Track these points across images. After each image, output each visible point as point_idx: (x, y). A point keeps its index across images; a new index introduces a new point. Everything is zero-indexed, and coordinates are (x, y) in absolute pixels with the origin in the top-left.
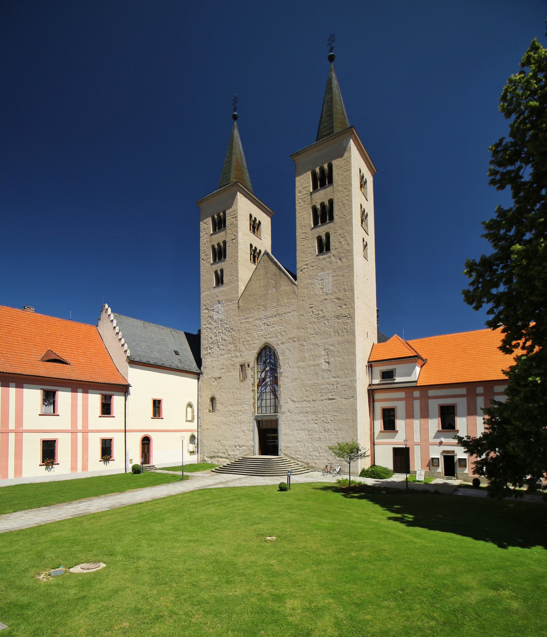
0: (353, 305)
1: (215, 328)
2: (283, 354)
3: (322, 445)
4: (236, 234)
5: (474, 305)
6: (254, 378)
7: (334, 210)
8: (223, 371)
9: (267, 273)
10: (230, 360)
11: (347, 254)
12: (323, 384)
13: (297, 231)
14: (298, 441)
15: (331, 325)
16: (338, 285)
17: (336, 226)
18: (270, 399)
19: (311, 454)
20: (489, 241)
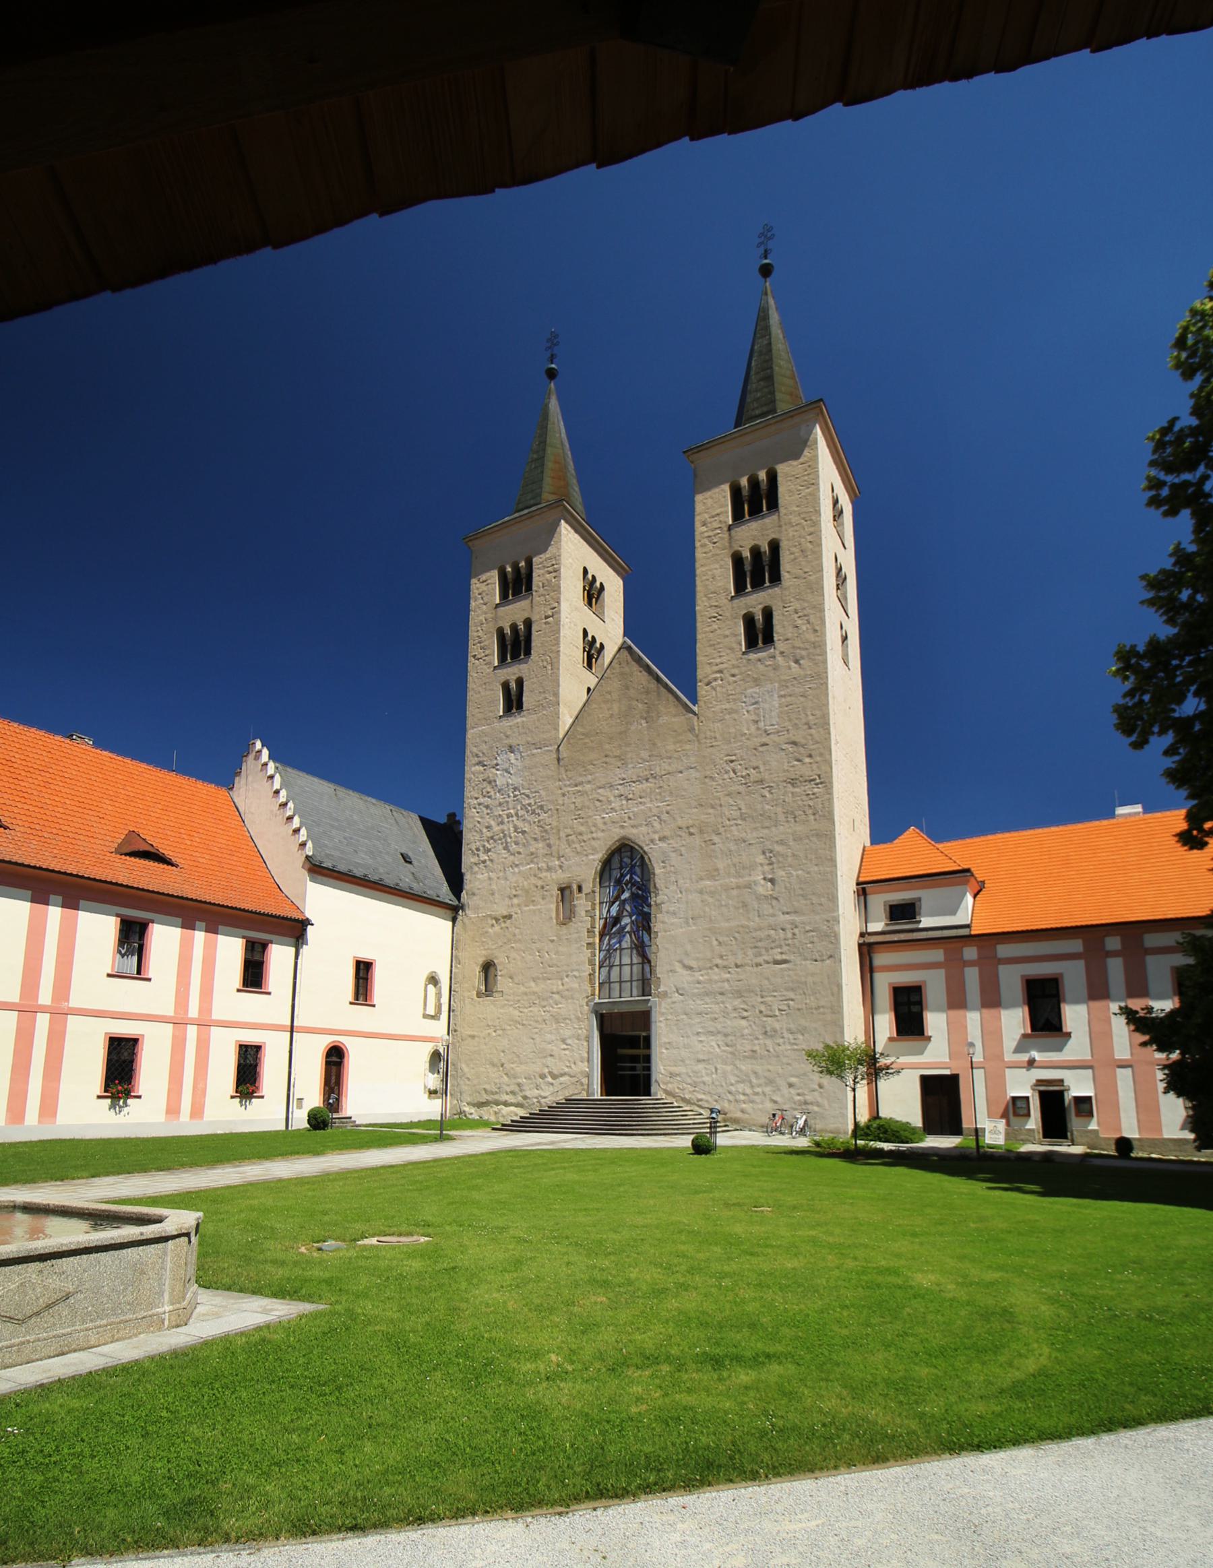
0: (828, 757)
1: (500, 804)
2: (663, 862)
3: (758, 1068)
4: (556, 605)
5: (1133, 738)
6: (593, 917)
7: (781, 562)
8: (515, 901)
9: (627, 688)
10: (535, 876)
11: (811, 651)
12: (760, 929)
13: (699, 602)
14: (699, 1061)
15: (776, 800)
16: (793, 716)
17: (787, 593)
18: (632, 964)
19: (733, 1089)
20: (1156, 611)
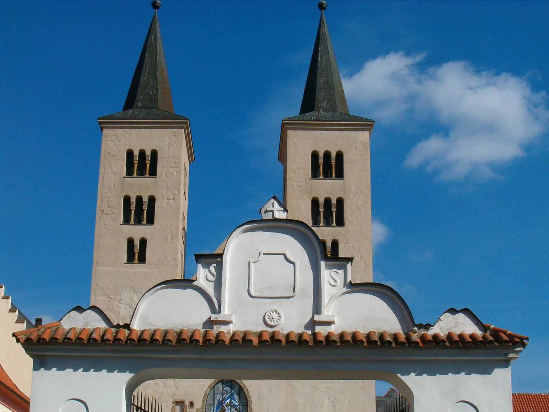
4: (177, 192)
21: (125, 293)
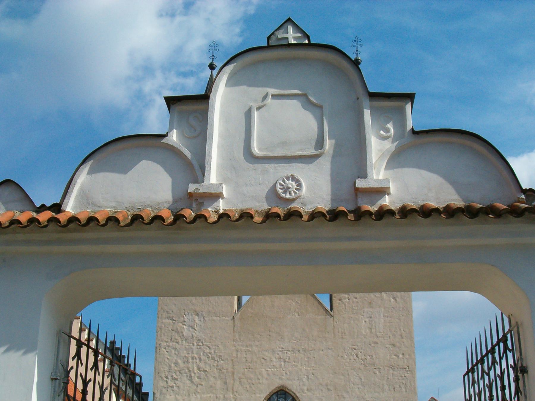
21: (188, 316)
